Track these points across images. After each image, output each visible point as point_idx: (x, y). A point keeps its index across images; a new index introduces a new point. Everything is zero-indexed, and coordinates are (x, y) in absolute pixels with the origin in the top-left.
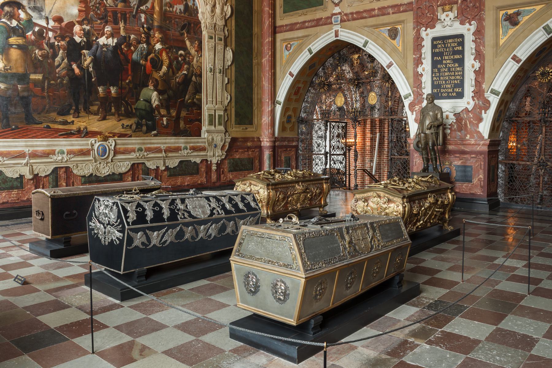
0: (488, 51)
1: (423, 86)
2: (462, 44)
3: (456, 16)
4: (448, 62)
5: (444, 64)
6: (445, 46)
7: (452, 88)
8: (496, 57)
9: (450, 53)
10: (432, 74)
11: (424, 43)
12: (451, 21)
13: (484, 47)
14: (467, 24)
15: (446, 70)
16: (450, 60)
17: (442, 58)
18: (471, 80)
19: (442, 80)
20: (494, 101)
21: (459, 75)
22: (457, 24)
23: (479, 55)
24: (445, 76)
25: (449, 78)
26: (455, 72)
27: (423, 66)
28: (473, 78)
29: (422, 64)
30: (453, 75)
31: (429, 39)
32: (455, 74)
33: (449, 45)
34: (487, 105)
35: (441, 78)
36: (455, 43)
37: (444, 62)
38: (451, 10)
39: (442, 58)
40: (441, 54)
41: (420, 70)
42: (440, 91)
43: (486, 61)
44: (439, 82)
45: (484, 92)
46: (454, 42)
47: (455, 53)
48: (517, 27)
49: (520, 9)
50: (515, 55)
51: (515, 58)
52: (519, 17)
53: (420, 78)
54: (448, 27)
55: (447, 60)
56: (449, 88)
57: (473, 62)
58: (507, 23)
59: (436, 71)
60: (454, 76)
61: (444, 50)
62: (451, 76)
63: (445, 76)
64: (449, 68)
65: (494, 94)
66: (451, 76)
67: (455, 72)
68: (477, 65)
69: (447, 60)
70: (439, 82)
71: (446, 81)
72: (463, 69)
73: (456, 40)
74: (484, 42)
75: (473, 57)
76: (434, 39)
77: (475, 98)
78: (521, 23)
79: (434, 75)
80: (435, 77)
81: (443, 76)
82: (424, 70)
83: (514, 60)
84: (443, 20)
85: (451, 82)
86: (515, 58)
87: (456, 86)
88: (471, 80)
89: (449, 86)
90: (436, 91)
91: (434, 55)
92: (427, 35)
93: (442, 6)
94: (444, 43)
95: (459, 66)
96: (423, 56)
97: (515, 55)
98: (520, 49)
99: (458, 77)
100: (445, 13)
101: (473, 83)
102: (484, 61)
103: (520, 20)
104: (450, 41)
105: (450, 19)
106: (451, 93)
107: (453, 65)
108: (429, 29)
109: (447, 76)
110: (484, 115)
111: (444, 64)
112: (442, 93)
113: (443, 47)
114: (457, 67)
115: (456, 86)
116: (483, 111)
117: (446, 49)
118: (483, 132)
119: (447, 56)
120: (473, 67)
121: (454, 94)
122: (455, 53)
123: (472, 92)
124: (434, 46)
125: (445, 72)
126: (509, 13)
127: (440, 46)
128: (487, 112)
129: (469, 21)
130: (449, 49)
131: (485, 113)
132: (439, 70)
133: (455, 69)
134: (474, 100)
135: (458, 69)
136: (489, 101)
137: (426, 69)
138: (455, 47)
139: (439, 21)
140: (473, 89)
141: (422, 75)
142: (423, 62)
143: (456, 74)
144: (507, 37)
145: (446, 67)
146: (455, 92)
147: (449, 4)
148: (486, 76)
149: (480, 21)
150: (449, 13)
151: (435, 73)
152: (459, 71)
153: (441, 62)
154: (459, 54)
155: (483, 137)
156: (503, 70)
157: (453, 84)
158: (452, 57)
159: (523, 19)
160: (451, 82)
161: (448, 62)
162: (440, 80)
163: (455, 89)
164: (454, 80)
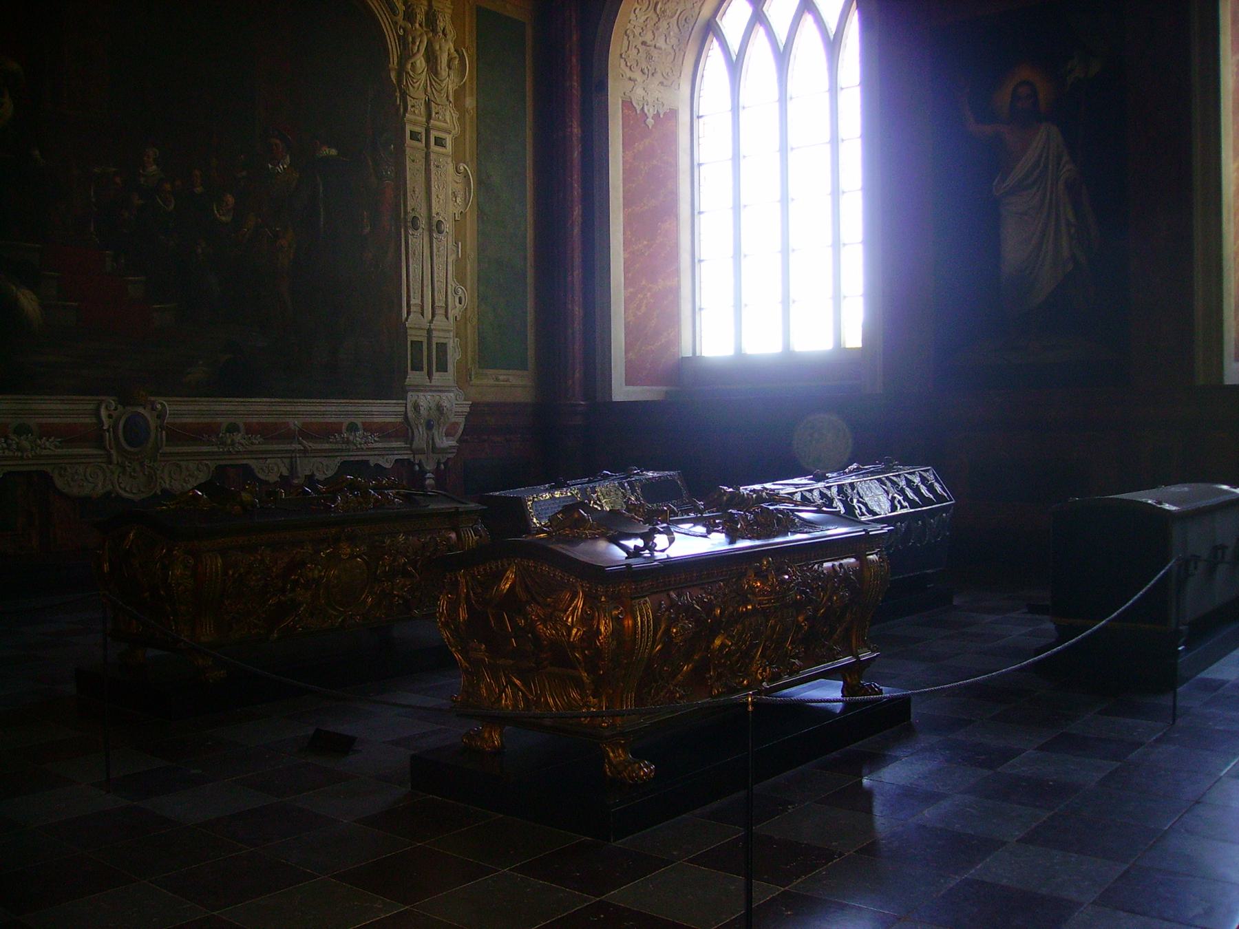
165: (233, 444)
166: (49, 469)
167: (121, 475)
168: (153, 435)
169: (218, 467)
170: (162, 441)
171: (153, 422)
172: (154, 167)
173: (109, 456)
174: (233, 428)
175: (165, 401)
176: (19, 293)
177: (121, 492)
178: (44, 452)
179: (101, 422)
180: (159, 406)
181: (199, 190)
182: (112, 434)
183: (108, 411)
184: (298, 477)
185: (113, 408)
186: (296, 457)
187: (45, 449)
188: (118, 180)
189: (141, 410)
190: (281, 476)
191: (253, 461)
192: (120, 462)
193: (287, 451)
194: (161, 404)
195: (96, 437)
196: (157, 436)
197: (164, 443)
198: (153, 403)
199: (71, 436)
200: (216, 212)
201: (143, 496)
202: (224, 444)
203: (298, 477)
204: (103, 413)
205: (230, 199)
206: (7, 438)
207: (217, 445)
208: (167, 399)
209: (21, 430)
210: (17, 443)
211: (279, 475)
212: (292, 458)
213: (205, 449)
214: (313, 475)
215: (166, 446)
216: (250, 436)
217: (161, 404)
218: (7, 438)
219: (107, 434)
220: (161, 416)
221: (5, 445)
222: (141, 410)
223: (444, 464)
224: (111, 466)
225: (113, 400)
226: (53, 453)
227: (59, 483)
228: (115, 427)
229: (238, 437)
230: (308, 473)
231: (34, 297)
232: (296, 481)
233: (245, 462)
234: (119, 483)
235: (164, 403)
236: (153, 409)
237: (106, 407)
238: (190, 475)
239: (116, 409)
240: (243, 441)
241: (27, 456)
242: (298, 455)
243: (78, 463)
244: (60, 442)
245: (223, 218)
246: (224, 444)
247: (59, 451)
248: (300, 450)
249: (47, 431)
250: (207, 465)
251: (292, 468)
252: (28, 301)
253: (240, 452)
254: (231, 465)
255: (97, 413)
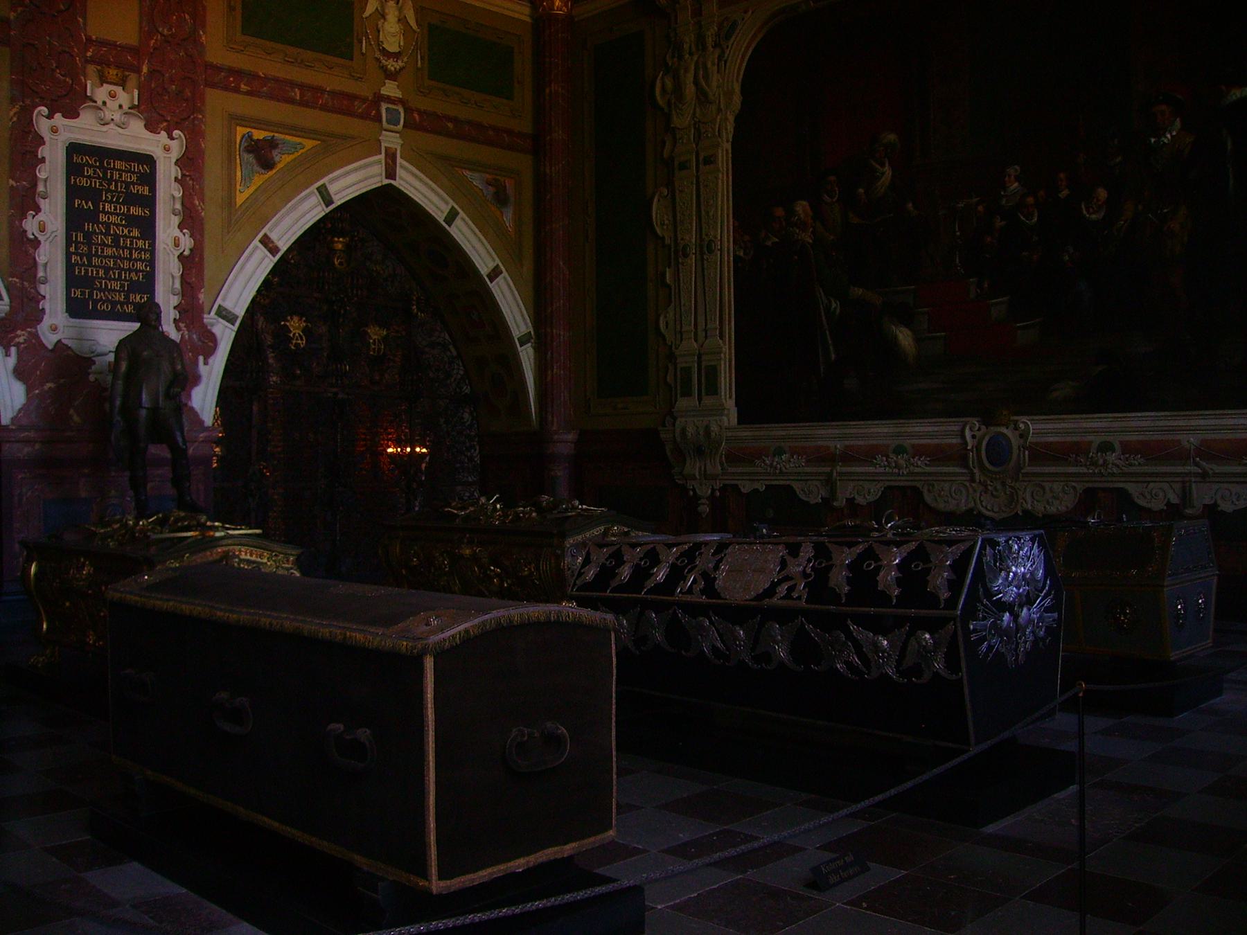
0: (211, 214)
1: (41, 274)
2: (149, 179)
3: (136, 103)
4: (113, 219)
5: (102, 224)
6: (105, 174)
7: (124, 291)
8: (229, 232)
9: (118, 198)
10: (68, 245)
11: (43, 152)
12: (120, 112)
13: (202, 200)
14: (164, 134)
15: (109, 241)
16: (118, 215)
17: (96, 205)
18: (173, 277)
19: (95, 266)
20: (225, 334)
21: (140, 260)
22: (137, 126)
23: (190, 220)
24: (105, 257)
25: (115, 263)
26: (131, 249)
27: (41, 217)
28: (178, 274)
29: (38, 210)
30: (126, 258)
31: (60, 144)
32: (131, 254)
33: (116, 176)
34: (208, 344)
35: (95, 261)
36: (134, 173)
37: (102, 218)
38: (122, 83)
39: (96, 205)
40: (94, 195)
41: (30, 225)
42: (91, 294)
43: (207, 237)
44: (87, 271)
45: (202, 312)
46: (129, 171)
47: (132, 199)
48: (271, 173)
49: (276, 135)
50: (265, 236)
51: (266, 241)
52: (275, 153)
53: (31, 251)
54: (112, 126)
55: (112, 214)
56: (115, 290)
57: (177, 233)
58: (250, 158)
59: (80, 238)
60: (130, 259)
61: (101, 185)
62: (122, 259)
63: (105, 257)
64: (116, 238)
65: (224, 318)
66: (120, 258)
67: (131, 249)
68: (187, 243)
69: (112, 214)
70: (87, 271)
71: (107, 269)
72: (153, 245)
73: (135, 166)
74: (202, 189)
75: (176, 220)
76: (74, 149)
77: (180, 324)
78: (280, 166)
79: (72, 249)
80: (76, 254)
81: (98, 257)
82: (42, 229)
83: (266, 247)
84: (100, 103)
85: (120, 275)
86: (266, 241)
87: (134, 287)
88: (173, 277)
89: (116, 285)
90: (78, 293)
91: (72, 192)
92: (54, 130)
93: (99, 64)
94: (101, 167)
95: (143, 237)
96: (41, 188)
97: (265, 236)
98: (276, 225)
99: (139, 265)
100: (107, 88)
101: (178, 285)
102: (202, 235)
103: (277, 159)
104: (118, 164)
105: (121, 107)
106: (122, 304)
107: (126, 231)
108: (58, 116)
109: (111, 257)
110: (203, 369)
111: (102, 224)
112: (95, 302)
113: (99, 178)
114: (138, 238)
115: (134, 287)
116: (201, 358)
117: (109, 185)
118: (202, 411)
119: (111, 202)
120: (177, 245)
121: (130, 309)
122: (132, 199)
123: (175, 308)
124: (73, 169)
125: (104, 244)
126: (255, 137)
127: (91, 172)
128: (210, 361)
129: (168, 125)
130: (116, 186)
131: (206, 363)
132: (88, 236)
133: (132, 243)
134: (178, 329)
135: (140, 243)
136: (213, 335)
137: (50, 228)
138: (134, 184)
139: (91, 104)
140: (175, 300)
141: (36, 243)
142: (42, 206)
143: (135, 255)
144: (251, 190)
145: (107, 234)
146: (132, 303)
147: (118, 67)
148: (208, 273)
149: (194, 137)
150: (119, 90)
151: (77, 242)
152: (142, 250)
153: (93, 216)
154: (143, 206)
155: (203, 422)
156: (242, 268)
157: (125, 280)
158: (124, 209)
159: (283, 160)
160: (120, 275)
161: (113, 219)
162: (90, 264)
163: (132, 297)
164: (130, 270)
165: (1105, 464)
166: (918, 485)
167: (983, 493)
168: (1015, 452)
169: (1088, 491)
170: (1024, 463)
171: (1015, 442)
172: (1016, 184)
173: (972, 474)
174: (1106, 447)
175: (1029, 420)
176: (898, 332)
177: (984, 511)
178: (917, 470)
179: (966, 444)
180: (1022, 426)
181: (1064, 193)
182: (975, 455)
183: (972, 432)
184: (1193, 507)
185: (977, 429)
186: (1190, 481)
187: (917, 467)
188: (980, 208)
189: (1004, 430)
190: (1169, 504)
191: (1129, 484)
192: (982, 480)
193: (1178, 474)
194: (1023, 422)
195: (960, 456)
196: (1019, 455)
197: (1026, 465)
198: (1016, 423)
199: (938, 455)
200: (1085, 212)
201: (1005, 515)
202: (1094, 464)
203: (1193, 507)
204: (968, 433)
205: (1102, 194)
206: (887, 457)
207: (1086, 466)
208: (1031, 417)
209: (899, 450)
210: (895, 462)
211: (1165, 502)
212: (1183, 482)
213: (1072, 470)
214: (1215, 505)
215: (1029, 466)
216: (1127, 456)
217: (1023, 422)
218: (887, 457)
219: (971, 454)
220: (1023, 436)
221: (886, 463)
222: (1004, 430)
223: (719, 490)
224: (974, 485)
225: (977, 421)
226: (923, 471)
227: (928, 498)
228: (978, 447)
229: (1112, 457)
230: (1207, 501)
231: (909, 333)
232: (1189, 511)
233: (1121, 485)
234: (981, 502)
235: (1029, 423)
236: (1016, 428)
237: (971, 429)
238: (1053, 497)
239: (979, 429)
240: (1118, 462)
241: (903, 473)
242: (1193, 479)
243: (943, 481)
244: (929, 461)
245: (1094, 216)
246: (1094, 464)
247: (928, 469)
248: (1196, 474)
249: (919, 451)
250: (1074, 488)
251: (1185, 495)
252: (904, 337)
253: (1114, 473)
254: (1104, 490)
255: (963, 436)
